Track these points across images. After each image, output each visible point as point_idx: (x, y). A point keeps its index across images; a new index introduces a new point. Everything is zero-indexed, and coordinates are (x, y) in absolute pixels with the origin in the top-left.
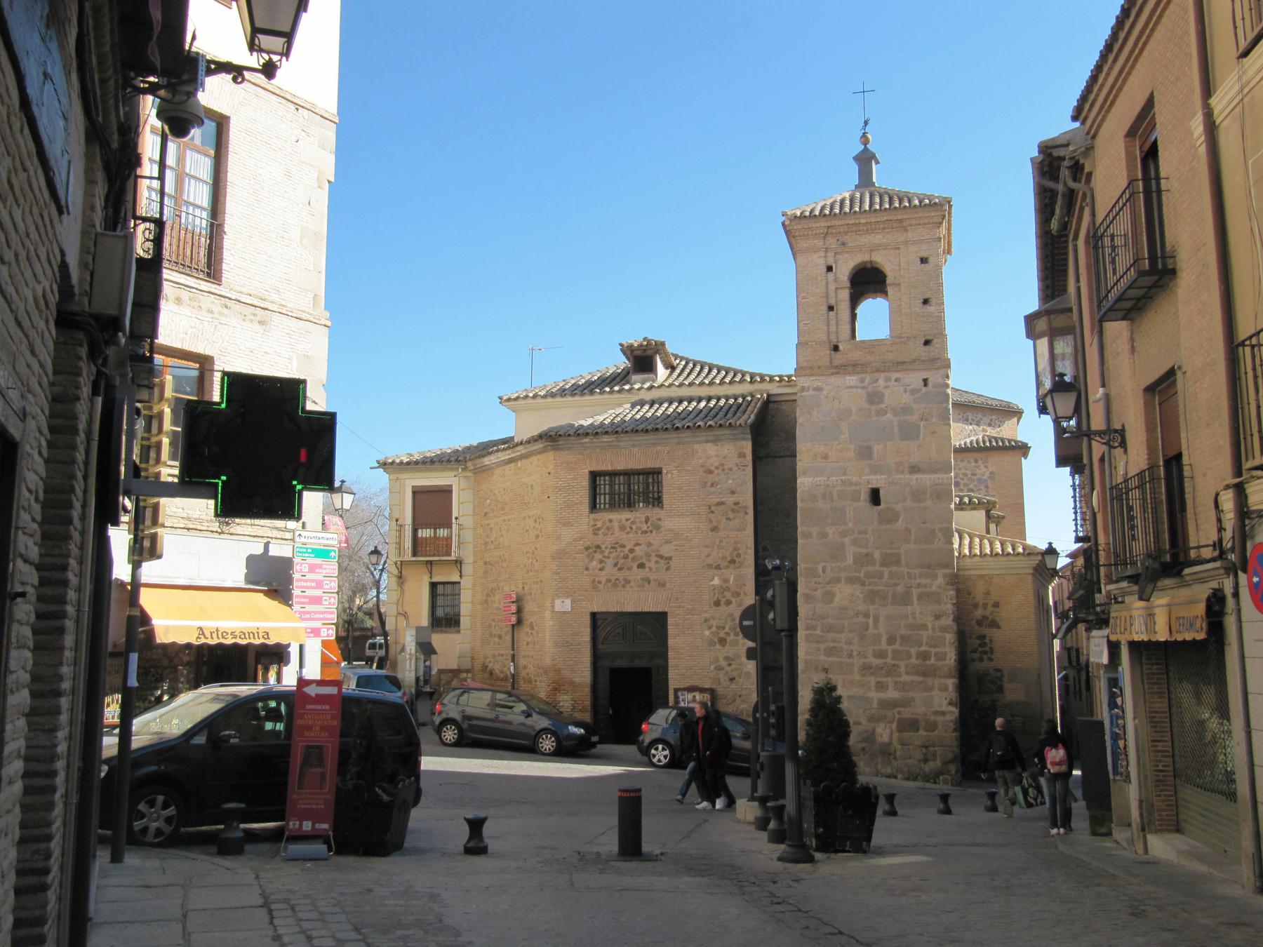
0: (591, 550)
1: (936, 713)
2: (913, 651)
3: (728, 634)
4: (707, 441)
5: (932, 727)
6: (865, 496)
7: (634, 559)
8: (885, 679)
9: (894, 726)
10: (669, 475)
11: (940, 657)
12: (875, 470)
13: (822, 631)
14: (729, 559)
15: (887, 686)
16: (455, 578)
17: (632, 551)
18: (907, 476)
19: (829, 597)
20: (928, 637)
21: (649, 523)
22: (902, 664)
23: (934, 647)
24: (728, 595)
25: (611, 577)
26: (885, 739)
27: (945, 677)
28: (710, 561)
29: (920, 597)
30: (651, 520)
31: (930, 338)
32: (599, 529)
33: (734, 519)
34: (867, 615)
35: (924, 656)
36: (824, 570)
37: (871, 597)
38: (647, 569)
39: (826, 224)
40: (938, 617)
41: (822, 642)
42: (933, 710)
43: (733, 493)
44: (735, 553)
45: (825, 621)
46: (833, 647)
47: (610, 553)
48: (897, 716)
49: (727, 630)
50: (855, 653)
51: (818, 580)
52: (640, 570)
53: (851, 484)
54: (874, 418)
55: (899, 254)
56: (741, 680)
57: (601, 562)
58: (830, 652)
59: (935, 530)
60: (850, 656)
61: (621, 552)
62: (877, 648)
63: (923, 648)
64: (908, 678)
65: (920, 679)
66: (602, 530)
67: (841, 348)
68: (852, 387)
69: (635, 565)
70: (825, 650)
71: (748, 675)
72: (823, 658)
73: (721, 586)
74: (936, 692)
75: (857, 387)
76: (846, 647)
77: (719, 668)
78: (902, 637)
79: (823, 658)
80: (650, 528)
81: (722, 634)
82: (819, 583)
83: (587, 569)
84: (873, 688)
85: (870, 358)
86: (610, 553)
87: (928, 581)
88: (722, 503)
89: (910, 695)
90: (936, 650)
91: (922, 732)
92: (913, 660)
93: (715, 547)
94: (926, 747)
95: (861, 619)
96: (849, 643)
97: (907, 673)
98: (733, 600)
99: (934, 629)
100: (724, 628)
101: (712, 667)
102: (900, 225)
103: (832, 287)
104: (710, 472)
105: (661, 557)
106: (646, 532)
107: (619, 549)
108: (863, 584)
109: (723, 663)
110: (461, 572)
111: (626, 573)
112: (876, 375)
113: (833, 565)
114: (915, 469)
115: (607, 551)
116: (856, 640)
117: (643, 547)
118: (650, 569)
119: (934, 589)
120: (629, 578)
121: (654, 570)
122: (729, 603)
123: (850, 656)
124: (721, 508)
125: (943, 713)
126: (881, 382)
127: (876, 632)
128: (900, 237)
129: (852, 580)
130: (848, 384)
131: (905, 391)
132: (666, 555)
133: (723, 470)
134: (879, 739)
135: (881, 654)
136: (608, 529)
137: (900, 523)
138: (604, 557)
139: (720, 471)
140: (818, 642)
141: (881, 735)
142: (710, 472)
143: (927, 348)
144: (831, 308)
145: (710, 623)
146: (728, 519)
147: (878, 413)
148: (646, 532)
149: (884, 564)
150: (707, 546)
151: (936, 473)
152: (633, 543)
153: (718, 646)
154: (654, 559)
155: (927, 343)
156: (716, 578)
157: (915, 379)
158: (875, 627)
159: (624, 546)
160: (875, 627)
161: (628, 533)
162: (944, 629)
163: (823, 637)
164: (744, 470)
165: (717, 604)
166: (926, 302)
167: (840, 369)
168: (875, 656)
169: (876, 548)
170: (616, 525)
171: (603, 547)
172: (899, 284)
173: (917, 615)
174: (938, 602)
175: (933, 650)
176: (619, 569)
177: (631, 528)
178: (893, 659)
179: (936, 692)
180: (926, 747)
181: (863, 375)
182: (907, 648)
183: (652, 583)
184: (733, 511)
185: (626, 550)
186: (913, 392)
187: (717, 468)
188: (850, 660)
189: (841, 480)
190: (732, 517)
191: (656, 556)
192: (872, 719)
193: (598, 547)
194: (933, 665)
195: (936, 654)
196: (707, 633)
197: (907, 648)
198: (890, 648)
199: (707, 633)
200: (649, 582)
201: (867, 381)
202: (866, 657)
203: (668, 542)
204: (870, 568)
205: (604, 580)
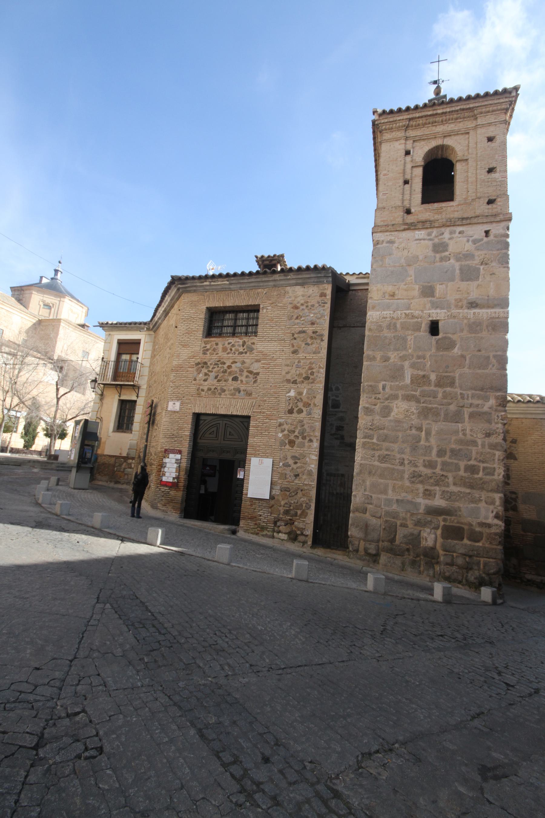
0: (200, 366)
1: (482, 524)
2: (462, 465)
3: (297, 437)
4: (297, 284)
5: (475, 537)
6: (425, 326)
7: (230, 373)
8: (433, 488)
9: (439, 532)
10: (265, 311)
11: (491, 472)
12: (435, 306)
13: (378, 439)
14: (304, 375)
15: (435, 494)
16: (134, 398)
17: (229, 367)
18: (466, 311)
19: (386, 411)
20: (477, 453)
21: (245, 347)
22: (450, 475)
23: (483, 462)
24: (300, 405)
25: (211, 387)
26: (430, 543)
27: (492, 491)
28: (289, 377)
29: (472, 416)
30: (247, 343)
31: (494, 198)
32: (208, 350)
33: (312, 344)
34: (420, 429)
35: (472, 469)
36: (384, 388)
37: (425, 413)
38: (239, 382)
39: (408, 117)
40: (488, 435)
41: (377, 450)
42: (479, 520)
43: (313, 324)
44: (310, 372)
45: (381, 432)
46: (387, 455)
47: (213, 368)
48: (442, 523)
49: (296, 434)
50: (406, 462)
51: (378, 396)
52: (234, 382)
53: (413, 317)
54: (438, 264)
55: (469, 138)
56: (304, 477)
57: (206, 374)
58: (383, 459)
59: (489, 357)
60: (402, 464)
61: (221, 367)
62: (427, 458)
63: (472, 462)
64: (455, 489)
65: (468, 491)
66: (210, 351)
67: (413, 210)
68: (420, 240)
69: (230, 378)
70: (379, 456)
71: (310, 473)
72: (377, 463)
73: (296, 398)
74: (482, 505)
75: (424, 239)
76: (398, 456)
77: (287, 465)
78: (452, 451)
79: (377, 463)
80: (246, 350)
81: (292, 437)
82: (379, 399)
83: (195, 380)
84: (421, 495)
85: (436, 217)
86: (213, 368)
87: (480, 402)
88: (304, 332)
89: (457, 504)
90: (485, 465)
91: (466, 541)
92: (462, 473)
93: (294, 366)
94: (470, 556)
95: (414, 431)
96: (401, 452)
97: (455, 484)
98: (304, 409)
99: (483, 446)
100: (294, 432)
101: (281, 464)
102: (471, 114)
103: (409, 166)
104: (296, 308)
105: (251, 372)
106: (242, 353)
107: (220, 366)
108: (418, 401)
109: (291, 462)
110: (138, 394)
111: (223, 383)
112: (443, 229)
113: (392, 384)
114: (473, 305)
115: (212, 366)
116: (408, 450)
117: (239, 365)
118: (242, 381)
119: (486, 409)
120: (225, 388)
121: (244, 382)
122: (300, 411)
123: (402, 464)
124: (302, 335)
125: (489, 526)
126: (447, 235)
127: (427, 444)
128: (470, 124)
129: (408, 398)
130: (417, 237)
131: (468, 241)
132: (255, 371)
133: (307, 306)
134: (423, 543)
135: (431, 465)
136: (214, 350)
137: (456, 350)
138: (209, 371)
139: (304, 307)
140: (374, 449)
141: (426, 540)
142: (296, 308)
143: (490, 206)
144: (406, 182)
145: (283, 427)
146: (307, 344)
147: (442, 259)
148: (242, 353)
149: (439, 384)
150: (288, 365)
151: (493, 308)
152: (231, 361)
153: (288, 447)
154: (245, 373)
155: (491, 202)
156: (292, 391)
157: (477, 231)
158: (427, 440)
159: (224, 363)
160: (427, 440)
161: (228, 353)
162: (494, 447)
163: (378, 445)
164: (324, 306)
165: (291, 412)
166: (491, 170)
167: (411, 227)
168: (425, 466)
169: (433, 371)
170: (220, 346)
171: (209, 363)
172: (467, 160)
173: (468, 432)
174: (489, 422)
175: (482, 465)
176: (219, 381)
177: (231, 350)
178: (442, 470)
179: (482, 505)
180: (470, 556)
181: (430, 230)
182: (456, 461)
183: (242, 392)
184: (312, 338)
185: (225, 366)
186: (475, 242)
187: (302, 305)
188: (401, 468)
189: (405, 313)
190: (310, 343)
191: (247, 371)
192: (418, 523)
193: (205, 363)
194: (481, 479)
195: (484, 469)
196: (280, 435)
197: (456, 461)
198: (439, 460)
199: (280, 435)
200: (239, 392)
201: (433, 235)
202: (416, 466)
203: (258, 361)
204: (426, 388)
205: (206, 388)
